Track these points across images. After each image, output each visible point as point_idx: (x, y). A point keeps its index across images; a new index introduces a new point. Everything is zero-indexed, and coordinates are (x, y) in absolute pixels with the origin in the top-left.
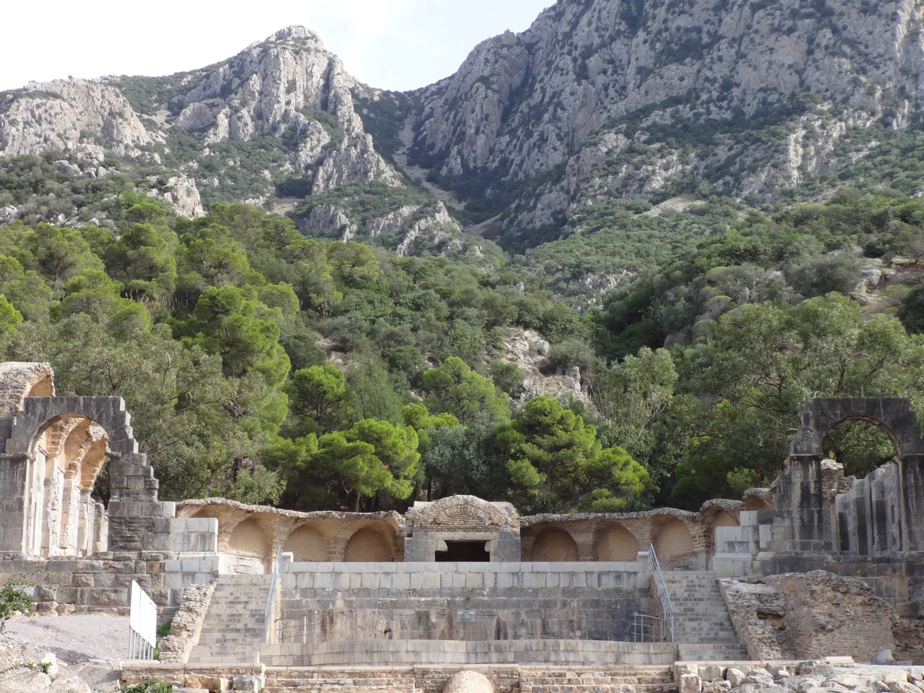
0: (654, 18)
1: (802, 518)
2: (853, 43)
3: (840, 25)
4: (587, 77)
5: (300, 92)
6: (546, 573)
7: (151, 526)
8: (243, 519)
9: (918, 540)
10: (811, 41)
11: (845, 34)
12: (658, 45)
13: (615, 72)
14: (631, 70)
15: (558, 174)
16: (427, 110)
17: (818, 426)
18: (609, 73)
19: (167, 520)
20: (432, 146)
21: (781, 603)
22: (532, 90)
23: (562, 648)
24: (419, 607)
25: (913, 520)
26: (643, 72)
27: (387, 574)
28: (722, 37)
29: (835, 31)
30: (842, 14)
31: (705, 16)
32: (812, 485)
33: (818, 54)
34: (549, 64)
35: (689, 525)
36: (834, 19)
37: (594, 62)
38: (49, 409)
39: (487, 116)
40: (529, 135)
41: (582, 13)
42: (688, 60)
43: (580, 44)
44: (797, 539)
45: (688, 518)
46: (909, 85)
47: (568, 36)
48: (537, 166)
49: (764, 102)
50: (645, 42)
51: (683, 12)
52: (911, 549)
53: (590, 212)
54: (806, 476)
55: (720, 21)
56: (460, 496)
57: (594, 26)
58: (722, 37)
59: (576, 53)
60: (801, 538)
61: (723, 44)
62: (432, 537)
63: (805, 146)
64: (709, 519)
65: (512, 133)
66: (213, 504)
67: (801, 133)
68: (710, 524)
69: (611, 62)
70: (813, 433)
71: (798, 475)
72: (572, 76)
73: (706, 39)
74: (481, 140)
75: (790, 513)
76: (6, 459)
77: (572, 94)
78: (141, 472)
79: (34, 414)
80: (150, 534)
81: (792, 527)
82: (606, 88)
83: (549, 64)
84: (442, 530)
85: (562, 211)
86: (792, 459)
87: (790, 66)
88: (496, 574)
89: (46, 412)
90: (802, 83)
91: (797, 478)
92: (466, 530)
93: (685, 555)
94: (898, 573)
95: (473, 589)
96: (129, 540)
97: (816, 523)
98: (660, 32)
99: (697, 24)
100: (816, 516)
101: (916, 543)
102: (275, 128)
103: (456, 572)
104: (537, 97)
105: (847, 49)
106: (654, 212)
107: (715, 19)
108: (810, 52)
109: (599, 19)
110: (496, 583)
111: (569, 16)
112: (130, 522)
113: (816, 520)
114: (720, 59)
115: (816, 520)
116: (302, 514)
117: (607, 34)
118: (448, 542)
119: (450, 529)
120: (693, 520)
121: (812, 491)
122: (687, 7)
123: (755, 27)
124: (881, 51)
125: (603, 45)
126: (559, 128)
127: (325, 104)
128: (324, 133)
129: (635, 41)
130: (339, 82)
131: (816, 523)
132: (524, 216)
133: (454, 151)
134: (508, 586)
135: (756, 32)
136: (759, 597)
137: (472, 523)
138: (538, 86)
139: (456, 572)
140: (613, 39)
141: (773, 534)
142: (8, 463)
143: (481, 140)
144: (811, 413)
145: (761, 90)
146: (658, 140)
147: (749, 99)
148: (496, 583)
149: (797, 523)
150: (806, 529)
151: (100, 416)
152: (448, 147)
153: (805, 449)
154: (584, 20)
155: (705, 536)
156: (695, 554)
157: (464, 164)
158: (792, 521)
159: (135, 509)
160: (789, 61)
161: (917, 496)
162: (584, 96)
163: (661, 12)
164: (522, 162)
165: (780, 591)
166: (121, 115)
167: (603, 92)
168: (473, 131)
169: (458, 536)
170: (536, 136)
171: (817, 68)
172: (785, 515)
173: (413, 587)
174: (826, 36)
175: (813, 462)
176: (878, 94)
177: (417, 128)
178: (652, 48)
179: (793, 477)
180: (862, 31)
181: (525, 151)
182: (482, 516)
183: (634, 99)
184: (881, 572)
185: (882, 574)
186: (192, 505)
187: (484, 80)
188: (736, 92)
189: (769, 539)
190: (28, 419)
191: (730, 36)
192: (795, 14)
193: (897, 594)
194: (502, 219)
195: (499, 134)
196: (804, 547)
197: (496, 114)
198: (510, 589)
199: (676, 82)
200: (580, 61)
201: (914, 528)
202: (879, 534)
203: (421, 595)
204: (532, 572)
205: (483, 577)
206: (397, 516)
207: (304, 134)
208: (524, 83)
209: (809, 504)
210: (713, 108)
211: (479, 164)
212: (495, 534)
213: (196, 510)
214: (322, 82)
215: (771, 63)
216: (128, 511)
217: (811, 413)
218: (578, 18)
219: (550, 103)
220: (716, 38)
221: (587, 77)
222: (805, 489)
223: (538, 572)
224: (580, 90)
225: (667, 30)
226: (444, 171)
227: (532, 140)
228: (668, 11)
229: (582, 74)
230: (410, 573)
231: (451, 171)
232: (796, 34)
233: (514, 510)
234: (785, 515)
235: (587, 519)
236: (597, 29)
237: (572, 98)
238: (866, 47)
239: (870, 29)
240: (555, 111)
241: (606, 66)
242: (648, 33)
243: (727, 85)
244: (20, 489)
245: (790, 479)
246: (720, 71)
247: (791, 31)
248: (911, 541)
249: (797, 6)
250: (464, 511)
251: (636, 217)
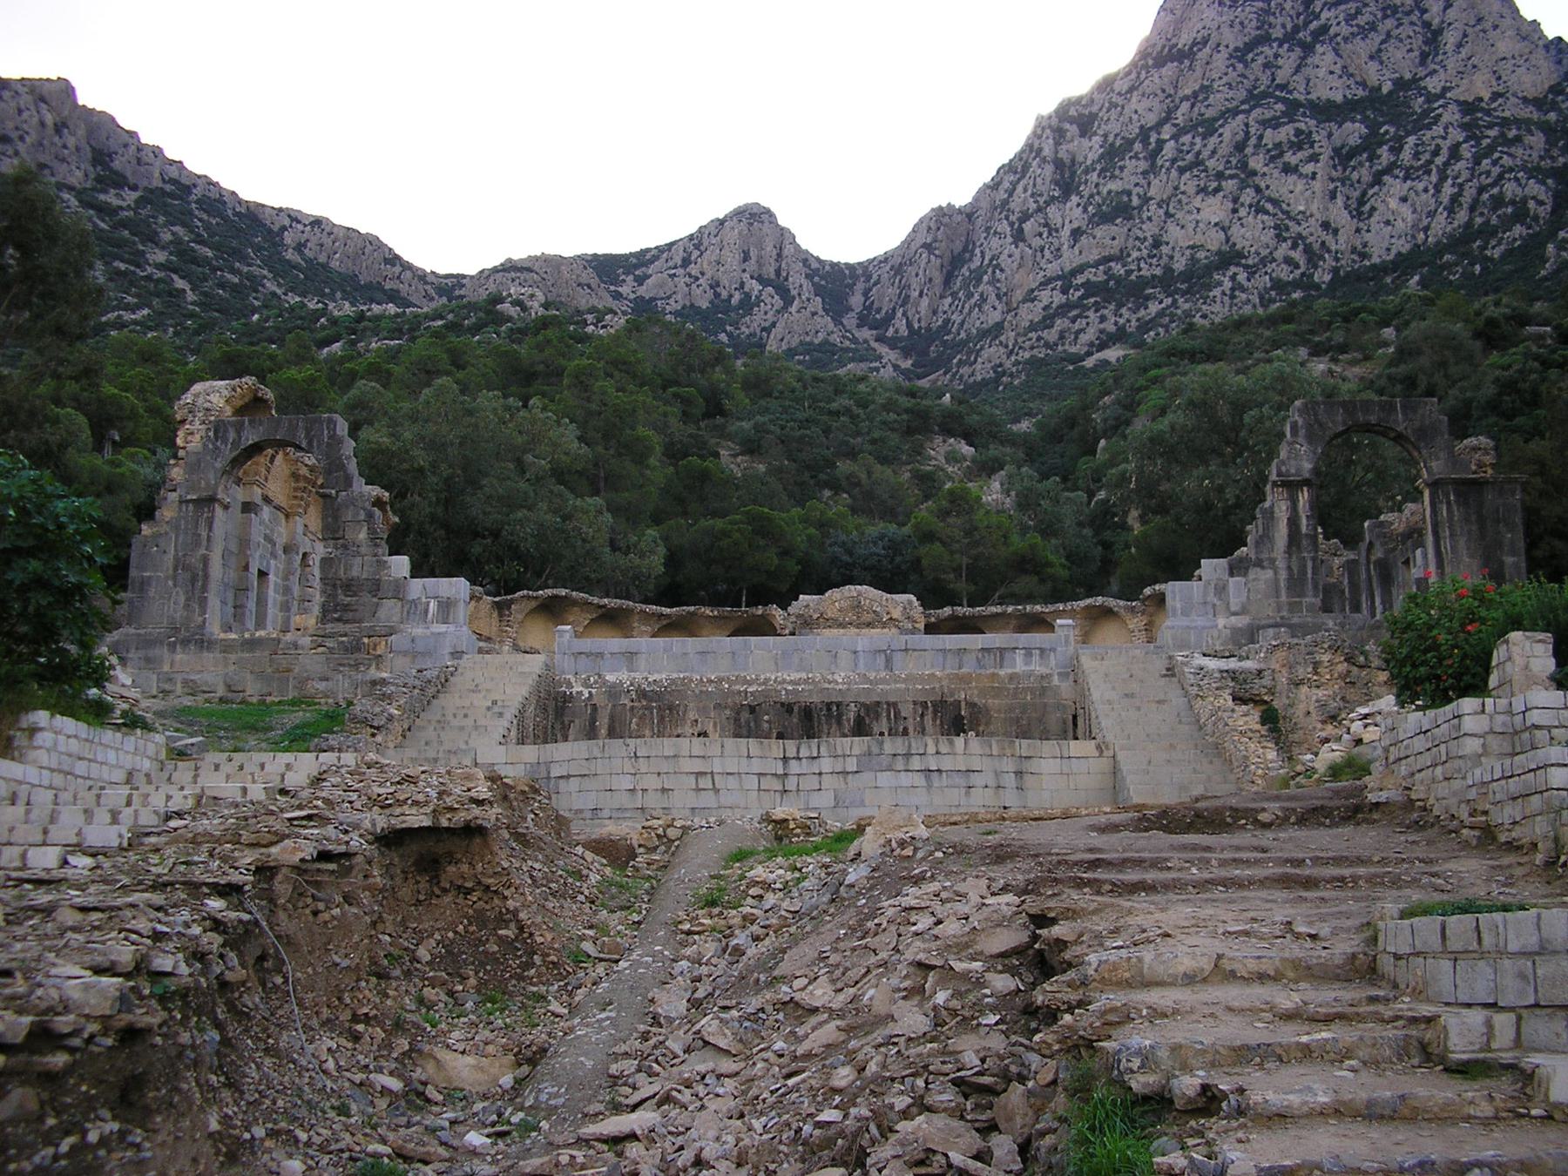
0: (1086, 182)
1: (1289, 568)
2: (1275, 202)
3: (1263, 185)
4: (1024, 240)
5: (753, 261)
7: (376, 587)
8: (595, 615)
10: (1235, 200)
11: (1267, 193)
12: (1090, 208)
13: (1050, 234)
14: (1066, 233)
15: (999, 328)
16: (875, 277)
17: (1311, 438)
18: (1045, 236)
19: (397, 580)
20: (879, 311)
21: (1266, 681)
22: (972, 254)
23: (931, 749)
26: (1076, 234)
28: (1151, 199)
29: (1258, 190)
30: (1265, 174)
31: (1134, 180)
32: (1304, 521)
33: (1243, 212)
34: (988, 229)
36: (1257, 179)
37: (1027, 226)
38: (245, 434)
39: (931, 280)
40: (970, 296)
41: (1019, 180)
42: (1118, 221)
43: (1018, 210)
44: (1284, 598)
45: (1126, 608)
46: (1329, 239)
47: (1005, 203)
48: (978, 323)
49: (1192, 258)
50: (1078, 205)
51: (1113, 177)
53: (1027, 362)
55: (1149, 184)
56: (852, 587)
57: (1029, 192)
58: (1151, 199)
59: (1013, 218)
61: (1153, 208)
63: (1233, 297)
65: (954, 295)
66: (556, 597)
67: (1228, 284)
69: (1046, 225)
70: (1303, 449)
72: (1010, 239)
73: (1135, 201)
74: (925, 302)
75: (1273, 561)
76: (188, 501)
77: (1010, 256)
78: (362, 516)
79: (225, 442)
80: (375, 600)
81: (1277, 581)
82: (1042, 250)
83: (988, 229)
85: (1001, 365)
86: (1275, 484)
87: (1216, 224)
89: (240, 438)
90: (1228, 240)
91: (1282, 511)
96: (346, 608)
97: (1309, 575)
98: (1092, 196)
99: (1127, 187)
100: (1310, 564)
102: (731, 296)
104: (977, 262)
105: (1269, 206)
106: (1089, 363)
107: (1143, 182)
108: (1235, 211)
109: (1034, 185)
111: (1006, 185)
112: (350, 586)
113: (1310, 571)
114: (1150, 219)
115: (1310, 571)
116: (668, 611)
117: (1041, 200)
121: (1304, 530)
122: (1117, 172)
123: (1183, 188)
124: (1302, 208)
125: (1039, 210)
126: (998, 289)
127: (778, 272)
128: (776, 297)
129: (1068, 204)
130: (788, 250)
131: (1309, 575)
132: (965, 370)
133: (899, 314)
135: (1183, 193)
136: (1233, 675)
137: (867, 617)
138: (977, 251)
140: (1047, 203)
142: (191, 507)
143: (925, 302)
144: (1300, 421)
145: (1192, 247)
146: (1093, 296)
147: (1177, 255)
149: (1283, 575)
150: (1296, 584)
151: (310, 443)
152: (894, 309)
153: (1293, 471)
154: (1020, 188)
157: (909, 325)
159: (355, 568)
160: (1215, 220)
162: (1022, 258)
163: (1094, 177)
164: (963, 322)
165: (1262, 666)
166: (589, 287)
167: (1039, 254)
168: (917, 293)
170: (977, 296)
171: (1242, 224)
174: (1248, 196)
175: (1305, 489)
176: (1301, 247)
177: (866, 294)
178: (1085, 210)
180: (1284, 190)
181: (966, 310)
183: (1070, 259)
186: (528, 597)
187: (926, 246)
188: (1165, 249)
190: (217, 448)
191: (1158, 199)
192: (1220, 176)
194: (945, 373)
195: (942, 297)
196: (1294, 608)
197: (938, 279)
199: (1108, 242)
200: (1016, 226)
202: (1383, 603)
206: (776, 613)
207: (759, 300)
208: (965, 249)
209: (1299, 547)
210: (1142, 265)
211: (923, 324)
213: (534, 604)
214: (775, 252)
215: (1197, 222)
216: (346, 570)
217: (1300, 421)
218: (1014, 185)
219: (988, 265)
220: (1146, 200)
221: (1024, 240)
222: (1293, 522)
224: (1017, 252)
225: (1098, 193)
226: (891, 330)
227: (973, 301)
228: (1099, 176)
229: (1019, 237)
231: (897, 331)
232: (1221, 194)
233: (916, 603)
236: (1032, 195)
237: (1010, 260)
238: (1288, 205)
239: (1291, 188)
240: (994, 272)
241: (1041, 229)
242: (1082, 197)
243: (1157, 244)
244: (204, 543)
245: (1272, 513)
246: (1150, 230)
247: (1217, 190)
249: (1221, 168)
250: (857, 606)
251: (1071, 368)
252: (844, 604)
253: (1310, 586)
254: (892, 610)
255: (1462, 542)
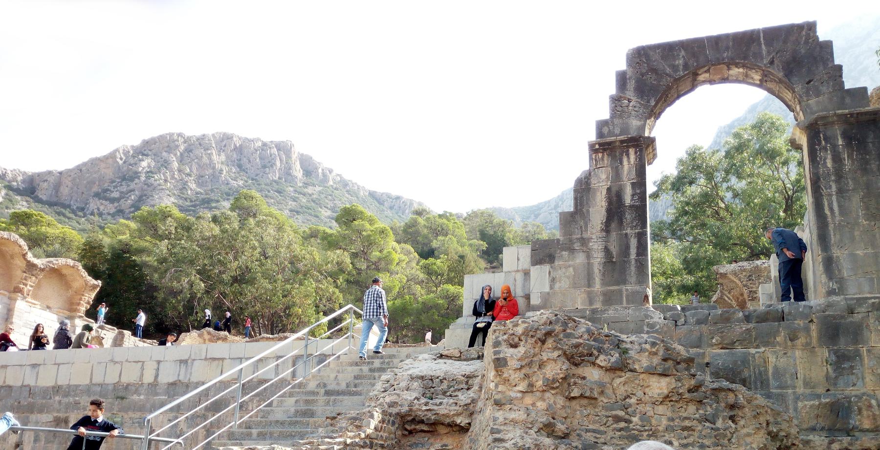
1: (607, 250)
6: (223, 359)
9: (845, 274)
24: (58, 411)
25: (833, 238)
27: (34, 366)
44: (598, 286)
52: (831, 293)
54: (617, 175)
60: (604, 283)
71: (604, 177)
75: (584, 242)
81: (589, 266)
88: (159, 362)
94: (801, 340)
95: (128, 385)
100: (633, 243)
101: (841, 281)
103: (112, 361)
110: (157, 376)
121: (628, 200)
134: (171, 380)
139: (112, 361)
141: (553, 281)
148: (157, 376)
149: (598, 258)
158: (589, 256)
161: (840, 192)
172: (577, 246)
173: (59, 383)
175: (632, 151)
179: (593, 181)
184: (766, 340)
185: (766, 344)
189: (547, 289)
193: (800, 383)
196: (610, 299)
198: (173, 384)
201: (836, 252)
203: (66, 395)
204: (206, 359)
205: (142, 369)
209: (621, 222)
223: (214, 359)
230: (59, 365)
234: (577, 246)
248: (830, 277)
253: (633, 268)
255: (856, 202)
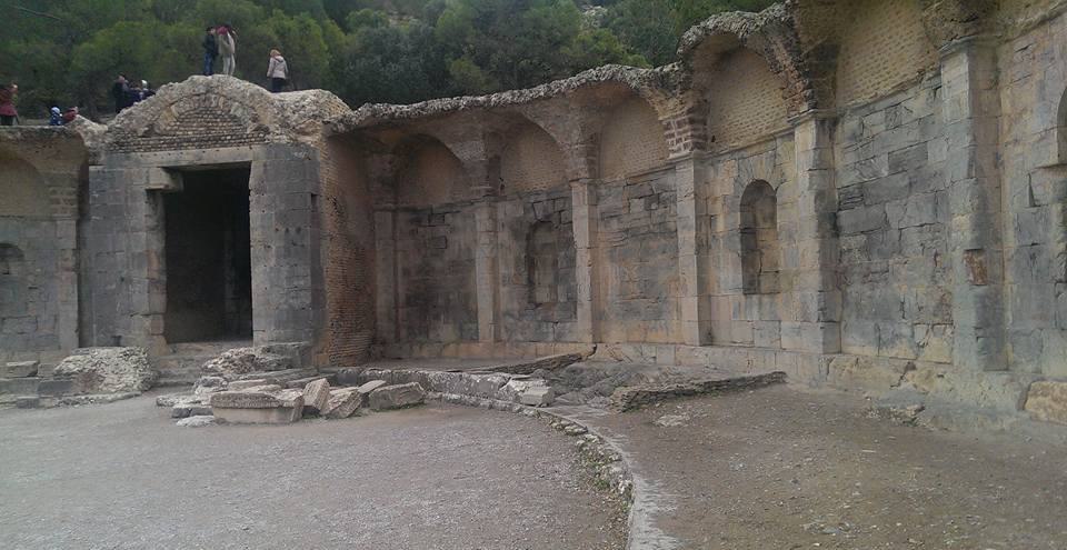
35: (654, 97)
62: (138, 163)
64: (701, 78)
68: (703, 91)
84: (156, 147)
92: (202, 143)
93: (652, 171)
118: (168, 170)
119: (170, 145)
120: (663, 83)
155: (692, 121)
156: (671, 167)
169: (188, 157)
182: (239, 114)
212: (257, 148)
235: (456, 108)
252: (186, 107)
254: (260, 112)
